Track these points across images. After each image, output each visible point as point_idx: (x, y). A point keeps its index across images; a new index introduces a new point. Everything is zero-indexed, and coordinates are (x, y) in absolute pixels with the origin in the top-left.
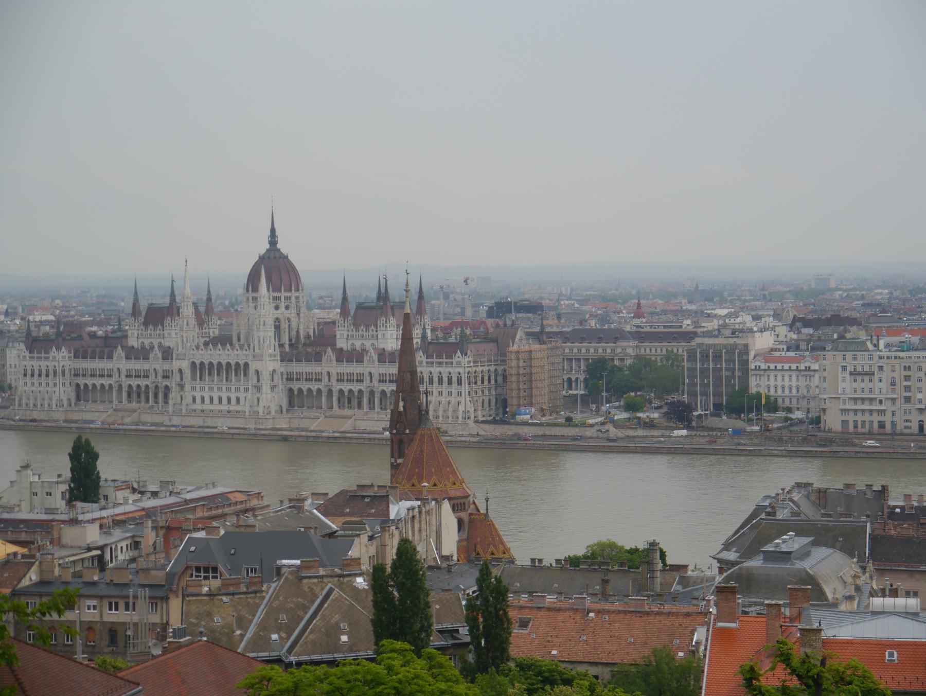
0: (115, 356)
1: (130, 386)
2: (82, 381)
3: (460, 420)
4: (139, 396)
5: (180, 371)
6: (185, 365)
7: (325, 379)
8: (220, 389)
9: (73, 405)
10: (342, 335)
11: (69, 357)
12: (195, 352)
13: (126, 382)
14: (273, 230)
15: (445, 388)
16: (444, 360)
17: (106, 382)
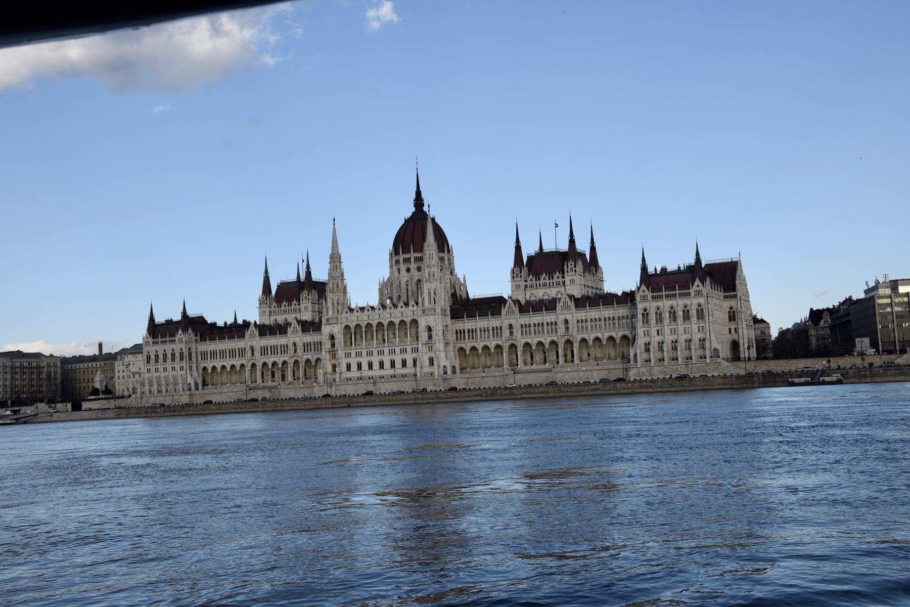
0: (247, 334)
1: (265, 364)
2: (209, 365)
3: (708, 360)
4: (273, 375)
5: (332, 337)
6: (337, 330)
7: (506, 333)
8: (381, 353)
9: (200, 387)
10: (518, 287)
11: (196, 340)
12: (349, 314)
13: (260, 360)
14: (418, 193)
15: (681, 325)
16: (677, 292)
17: (237, 362)
